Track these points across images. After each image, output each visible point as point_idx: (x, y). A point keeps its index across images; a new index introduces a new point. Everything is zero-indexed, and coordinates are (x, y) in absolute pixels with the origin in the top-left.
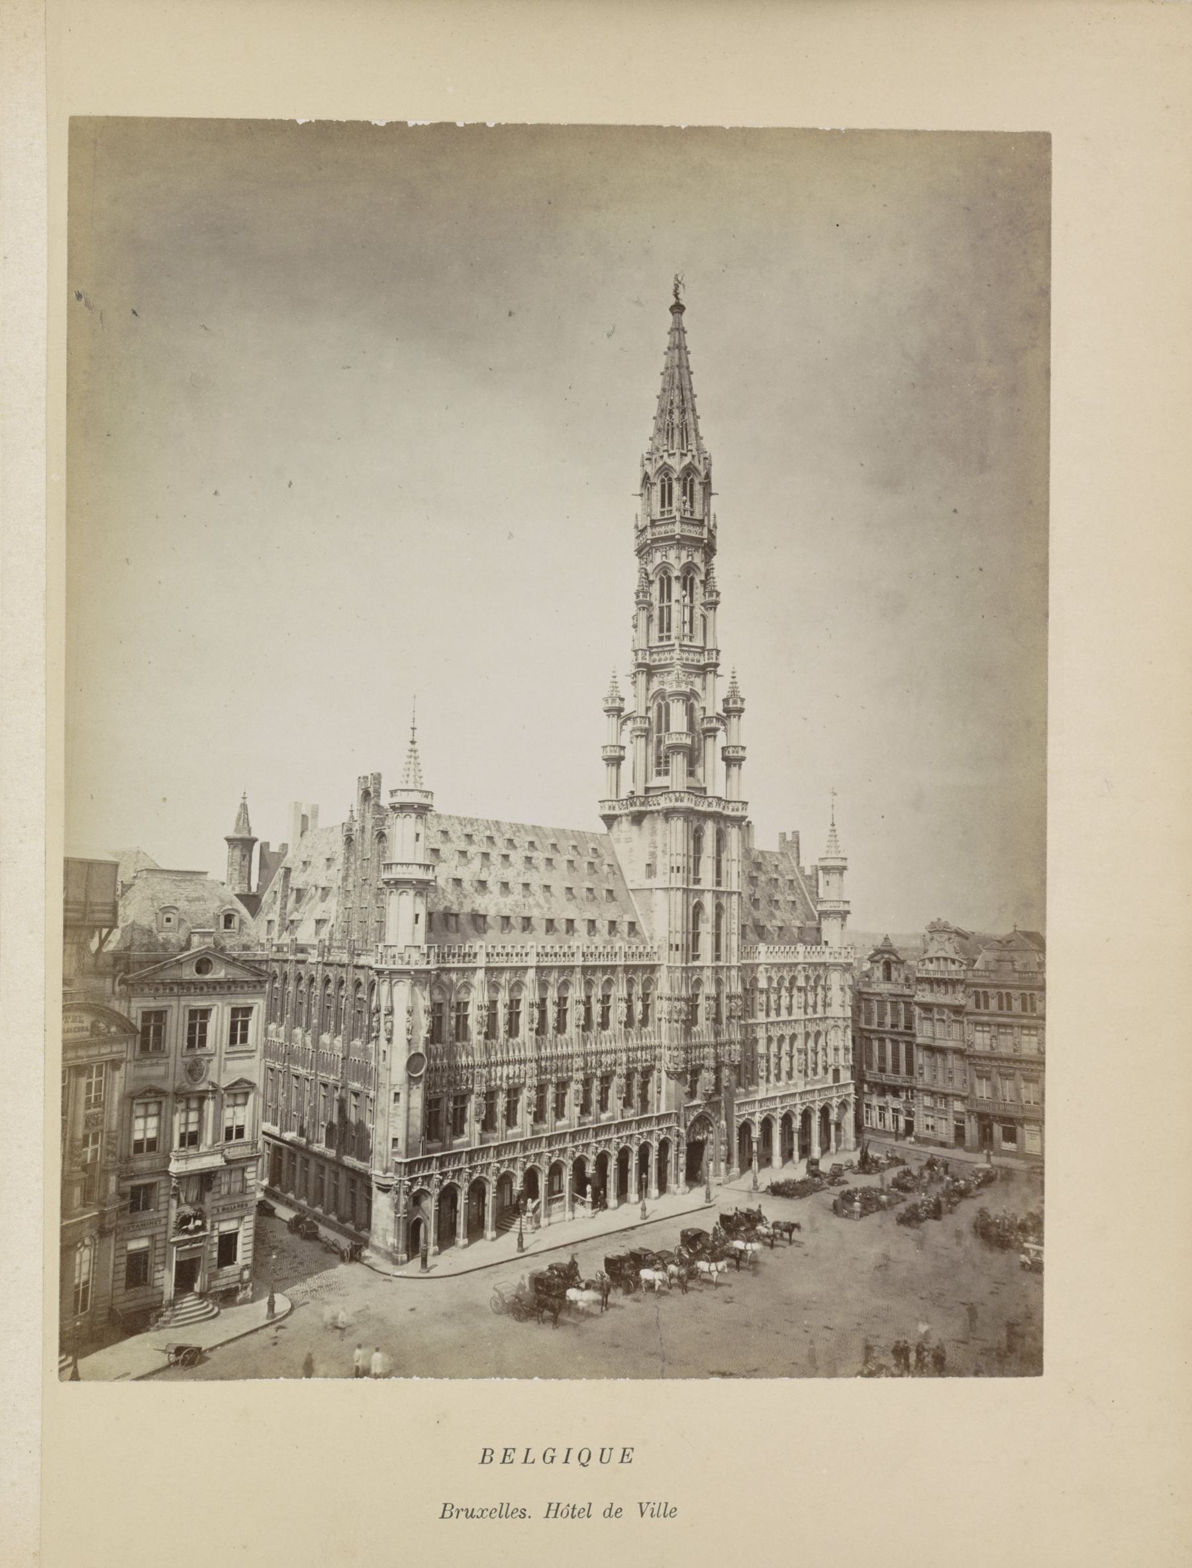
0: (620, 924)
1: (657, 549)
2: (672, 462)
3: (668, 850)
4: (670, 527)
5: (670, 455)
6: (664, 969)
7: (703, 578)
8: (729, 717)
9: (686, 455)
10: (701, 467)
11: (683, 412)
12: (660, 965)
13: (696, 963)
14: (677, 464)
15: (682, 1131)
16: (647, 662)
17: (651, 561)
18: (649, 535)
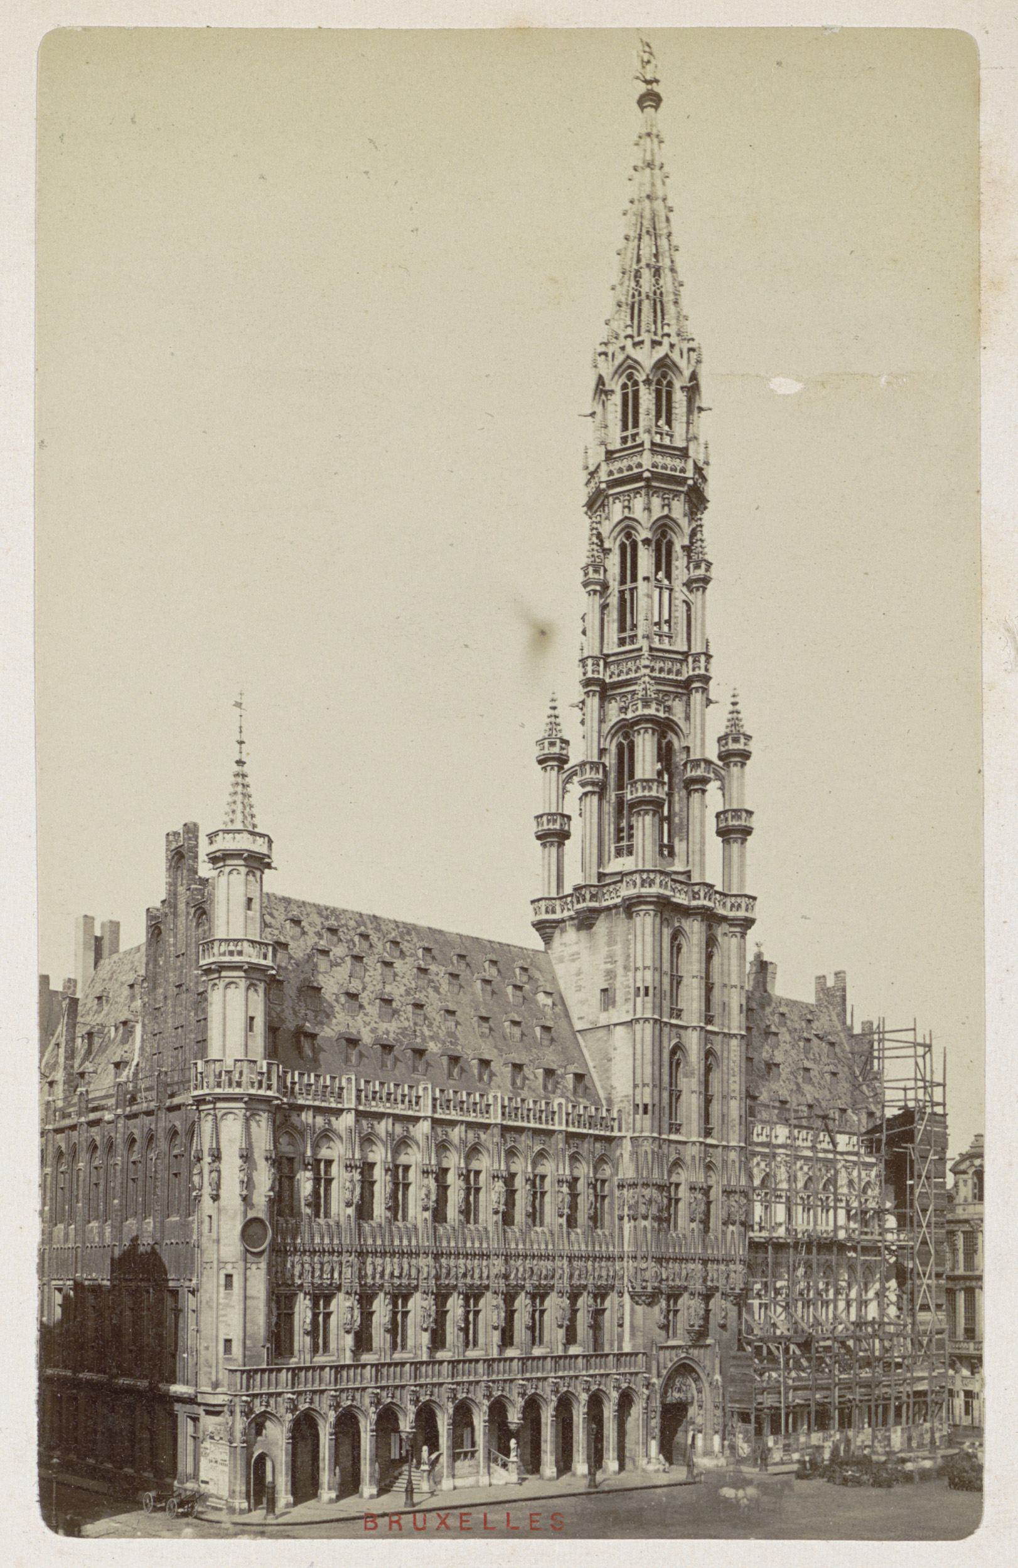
0: (563, 1077)
1: (616, 496)
2: (637, 354)
3: (632, 964)
4: (636, 460)
5: (635, 345)
6: (627, 1145)
7: (686, 542)
8: (727, 765)
9: (660, 343)
10: (682, 364)
11: (657, 272)
12: (621, 1138)
13: (673, 1137)
14: (647, 358)
15: (654, 1380)
16: (601, 676)
17: (607, 518)
18: (603, 476)
